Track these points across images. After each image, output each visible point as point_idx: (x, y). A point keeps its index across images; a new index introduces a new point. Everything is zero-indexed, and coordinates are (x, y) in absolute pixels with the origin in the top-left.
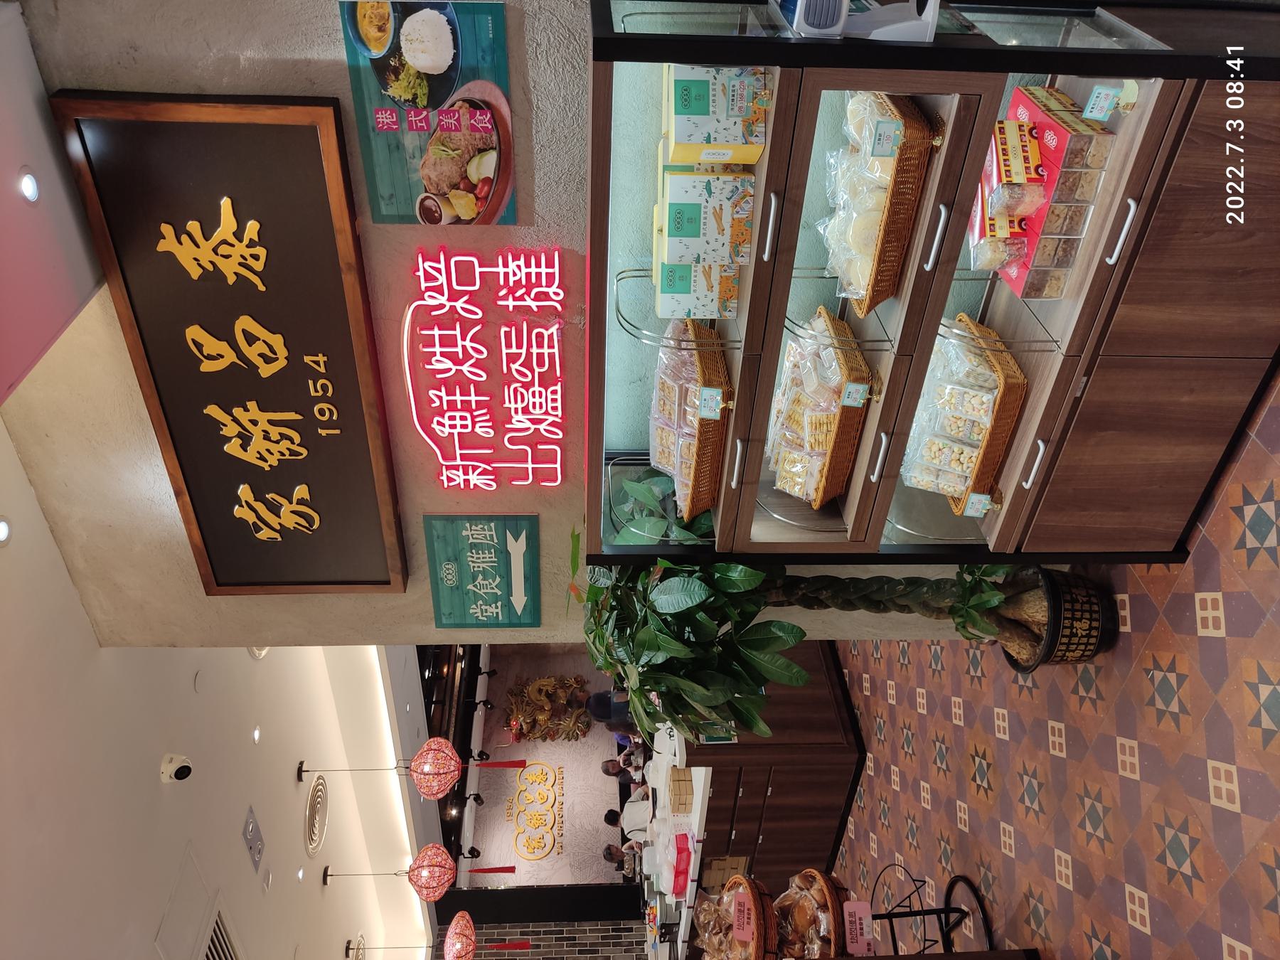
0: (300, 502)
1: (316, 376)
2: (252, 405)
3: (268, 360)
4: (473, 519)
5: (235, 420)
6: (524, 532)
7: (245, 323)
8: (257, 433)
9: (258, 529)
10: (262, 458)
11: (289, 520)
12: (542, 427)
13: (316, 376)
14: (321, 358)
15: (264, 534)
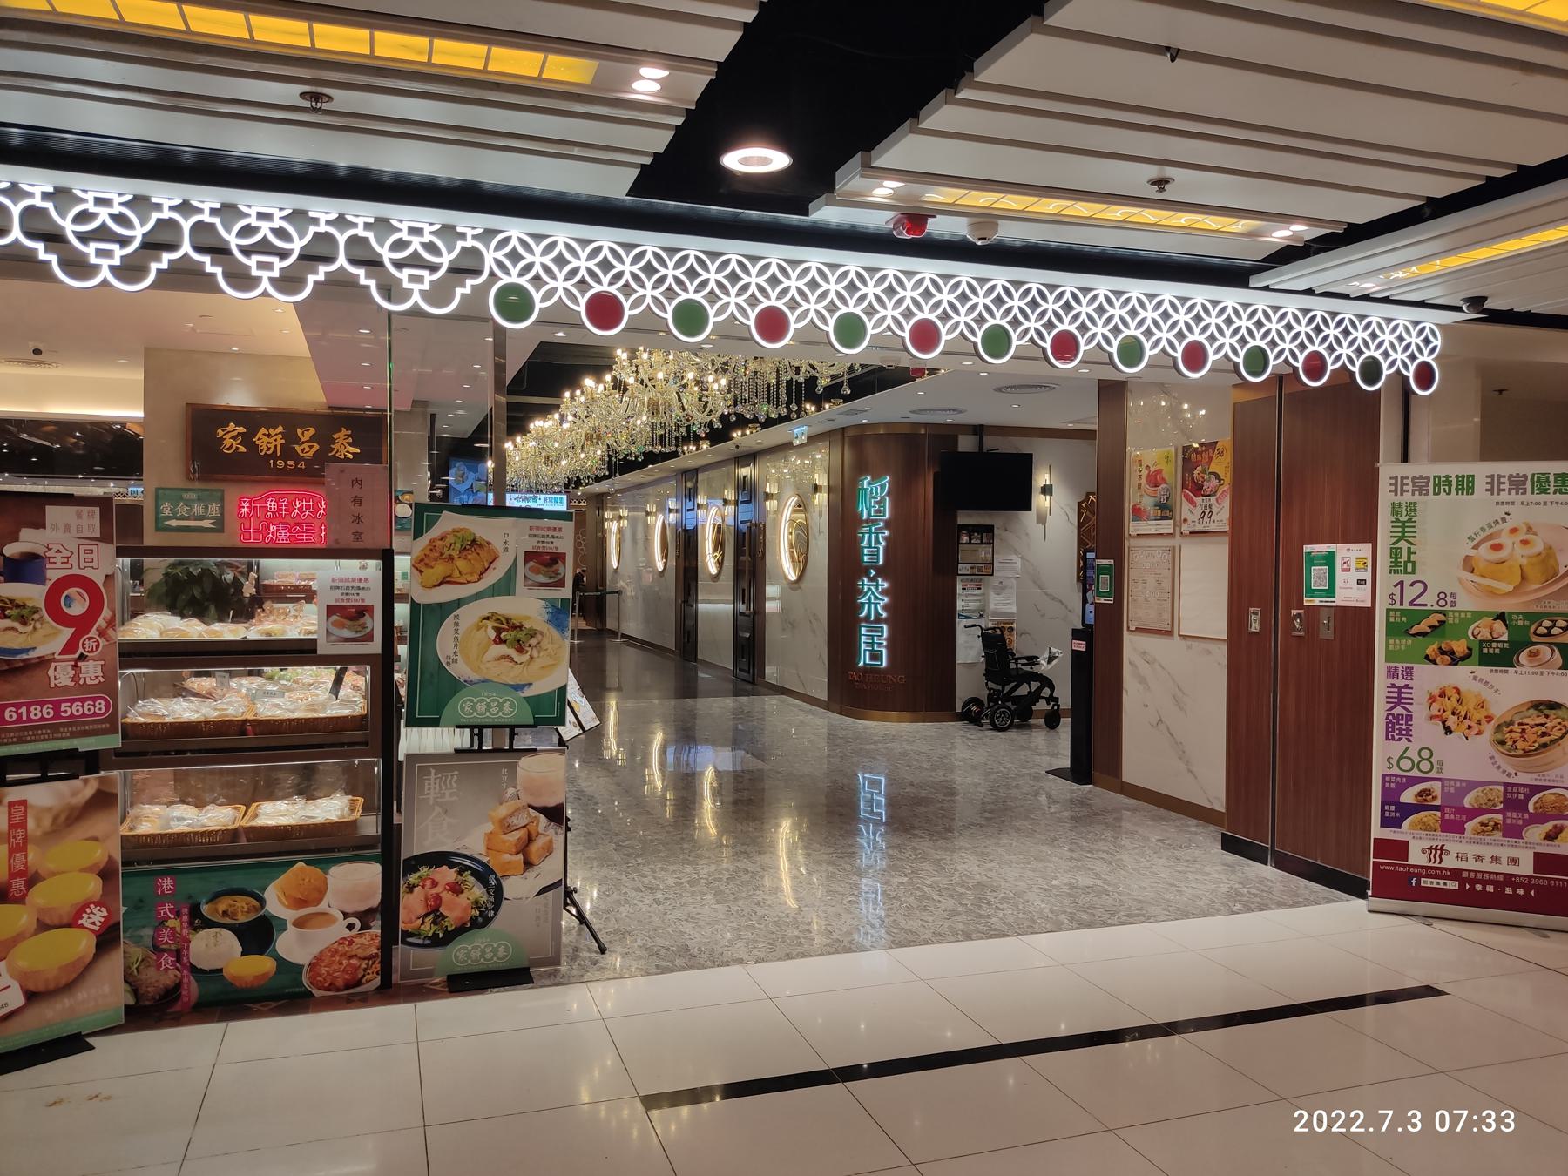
0: (237, 448)
1: (296, 464)
2: (283, 441)
3: (303, 450)
4: (222, 508)
5: (276, 434)
6: (166, 523)
7: (317, 447)
8: (272, 440)
9: (223, 430)
10: (259, 439)
11: (228, 442)
12: (270, 535)
13: (296, 464)
14: (303, 467)
15: (220, 432)
